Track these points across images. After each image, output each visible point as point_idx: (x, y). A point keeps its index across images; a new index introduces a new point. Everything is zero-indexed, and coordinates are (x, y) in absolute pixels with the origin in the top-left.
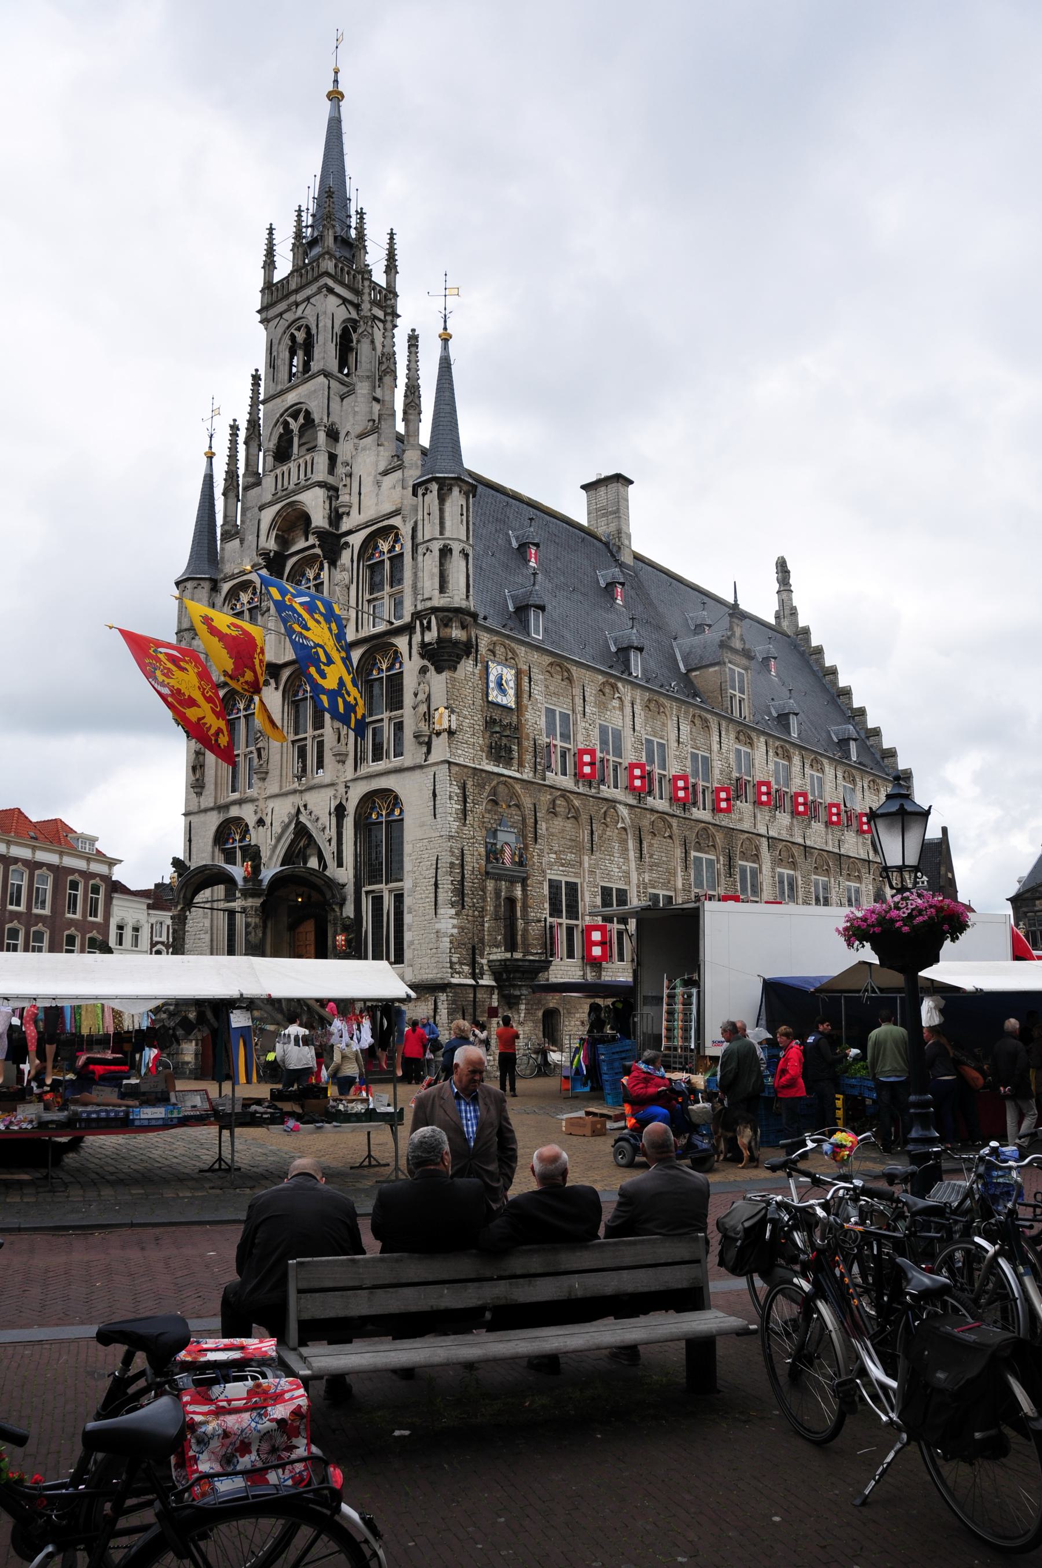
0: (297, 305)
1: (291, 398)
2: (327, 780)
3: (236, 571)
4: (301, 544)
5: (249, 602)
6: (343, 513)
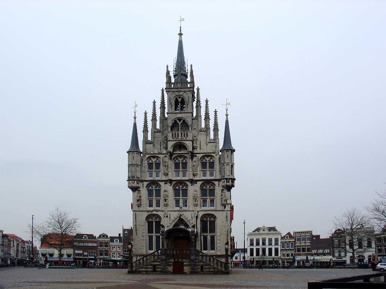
0: (181, 91)
1: (179, 116)
2: (190, 209)
3: (152, 153)
4: (178, 152)
5: (155, 161)
6: (195, 148)
